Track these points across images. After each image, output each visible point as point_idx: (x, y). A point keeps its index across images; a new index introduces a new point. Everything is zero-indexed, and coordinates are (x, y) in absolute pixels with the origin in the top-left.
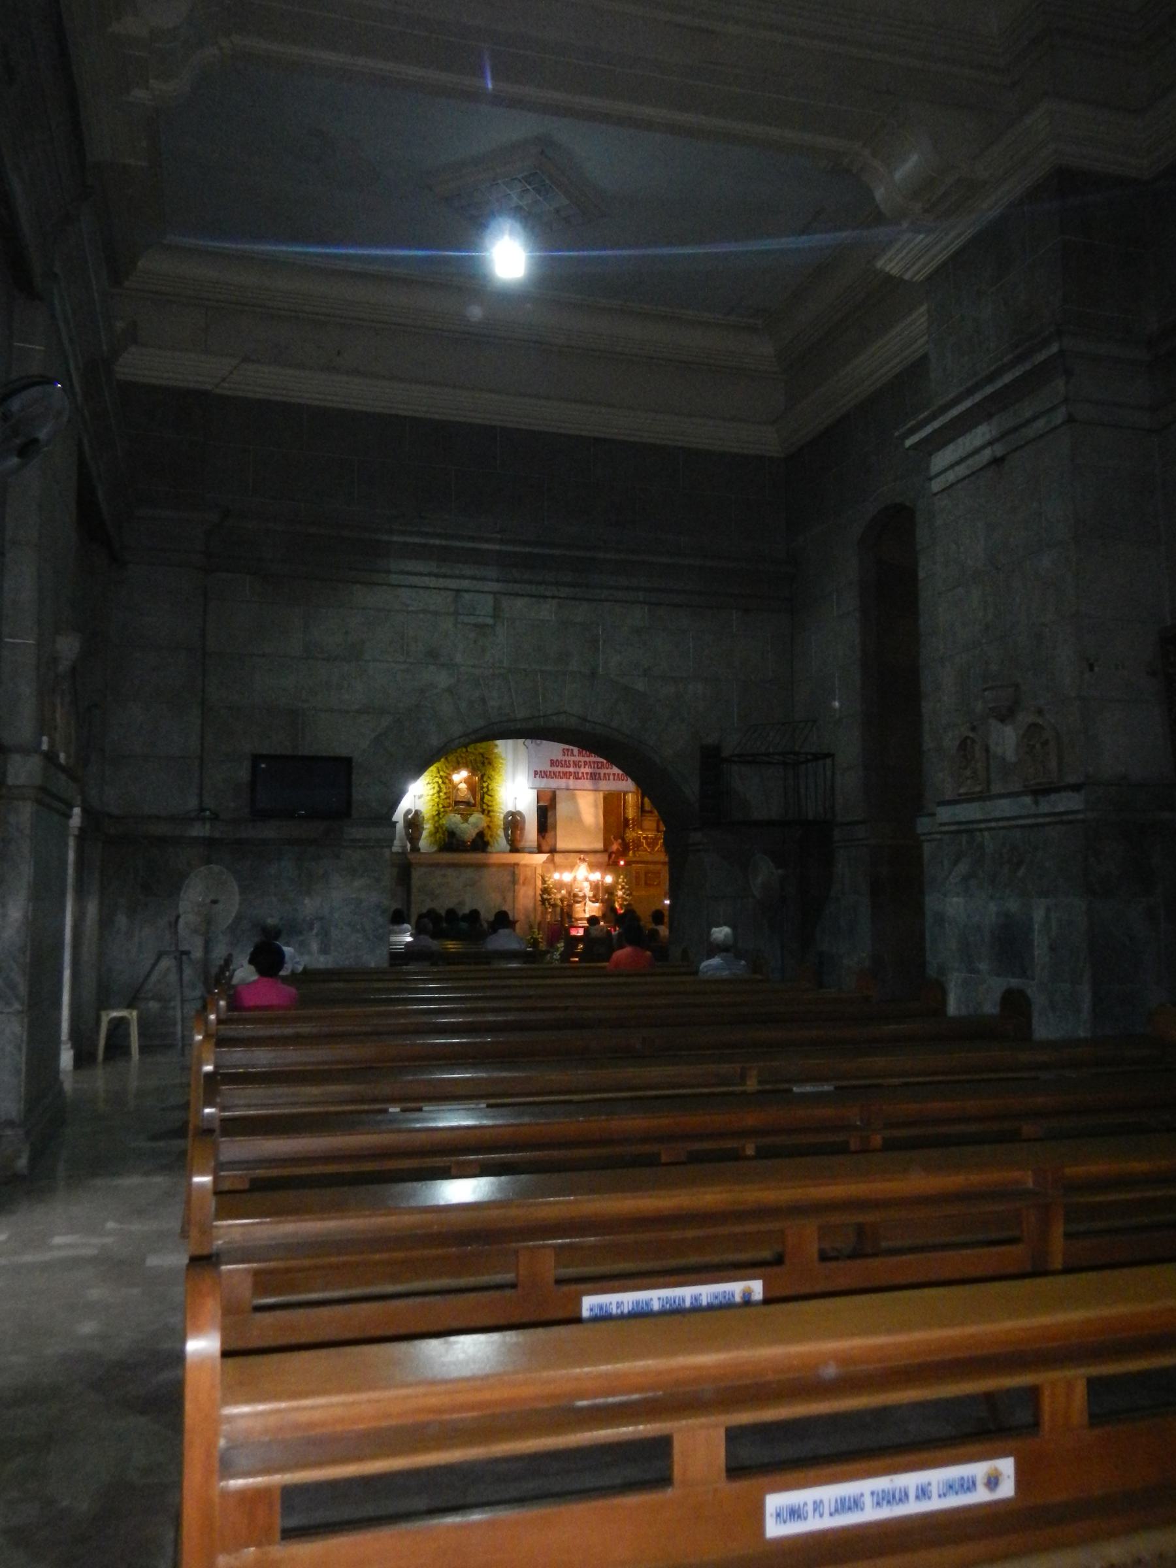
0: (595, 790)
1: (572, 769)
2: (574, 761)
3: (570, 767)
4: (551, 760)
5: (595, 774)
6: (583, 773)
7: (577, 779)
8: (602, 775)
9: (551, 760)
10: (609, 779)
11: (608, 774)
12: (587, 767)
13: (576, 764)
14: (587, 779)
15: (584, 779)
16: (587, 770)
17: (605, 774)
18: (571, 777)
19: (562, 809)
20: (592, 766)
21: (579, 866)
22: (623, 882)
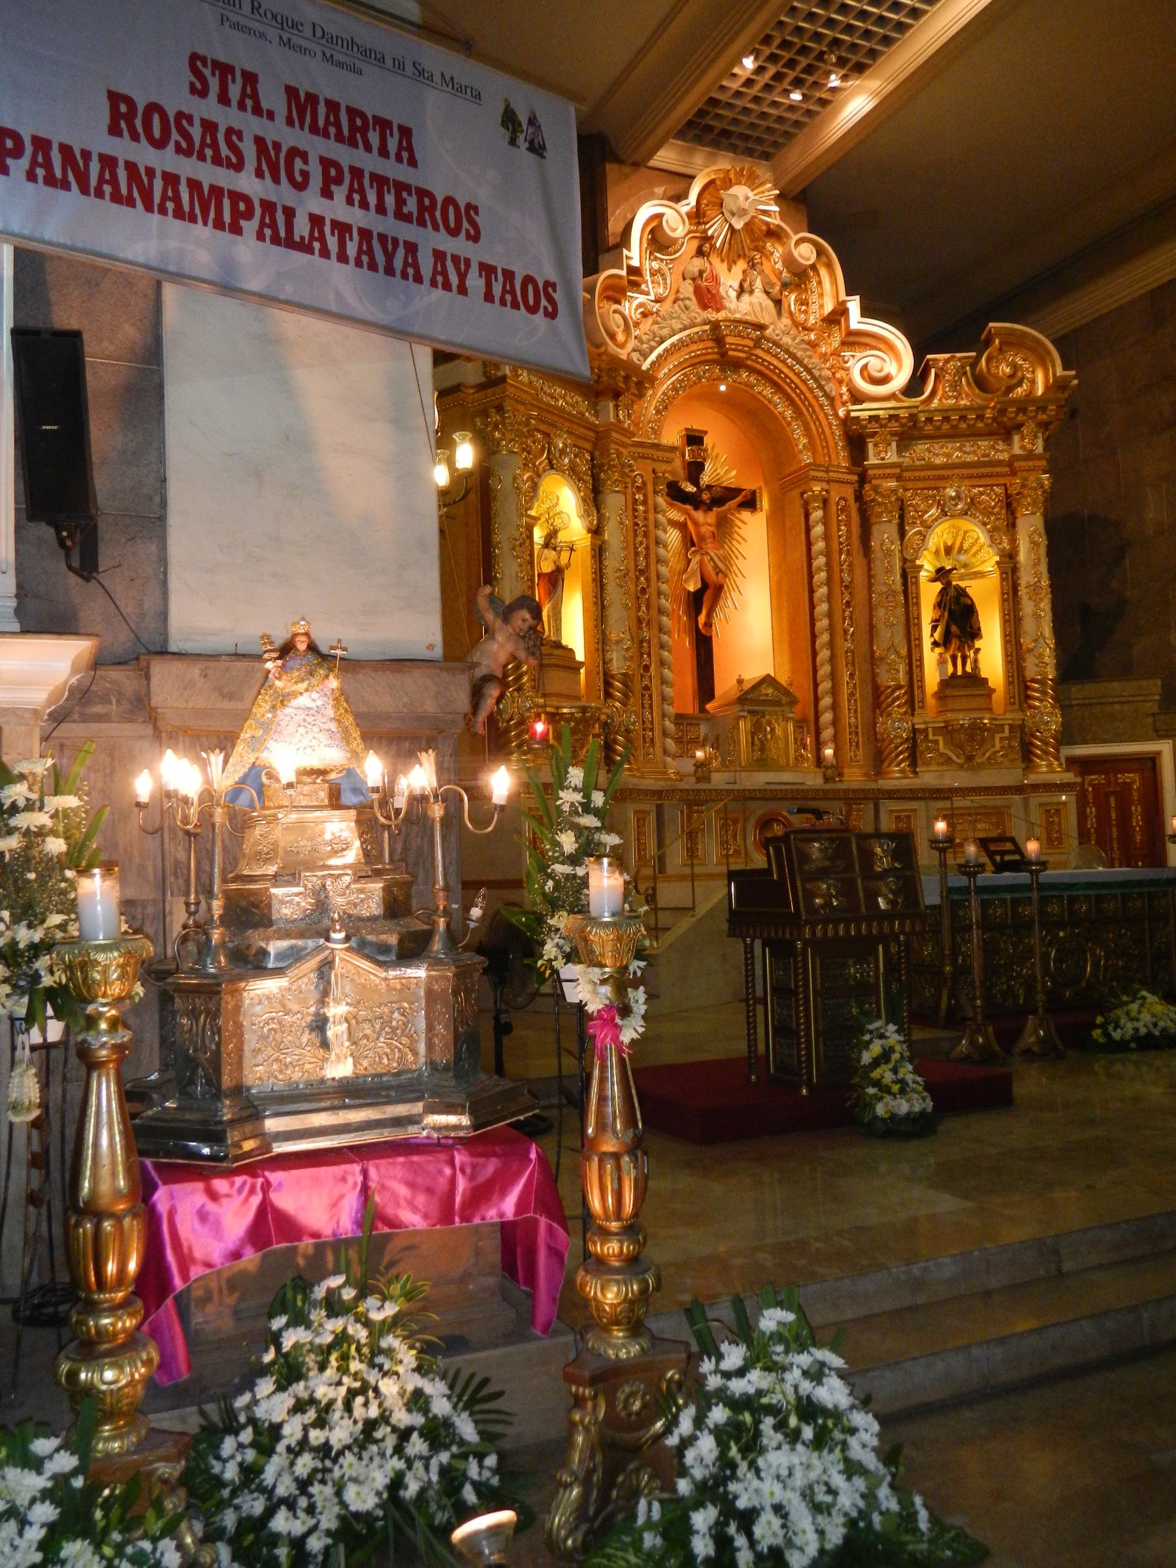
1: (248, 183)
2: (259, 141)
3: (239, 167)
4: (114, 98)
6: (316, 221)
7: (276, 240)
9: (114, 98)
10: (462, 290)
11: (456, 259)
12: (340, 193)
14: (343, 258)
15: (325, 253)
16: (337, 209)
18: (250, 227)
20: (372, 199)
21: (283, 699)
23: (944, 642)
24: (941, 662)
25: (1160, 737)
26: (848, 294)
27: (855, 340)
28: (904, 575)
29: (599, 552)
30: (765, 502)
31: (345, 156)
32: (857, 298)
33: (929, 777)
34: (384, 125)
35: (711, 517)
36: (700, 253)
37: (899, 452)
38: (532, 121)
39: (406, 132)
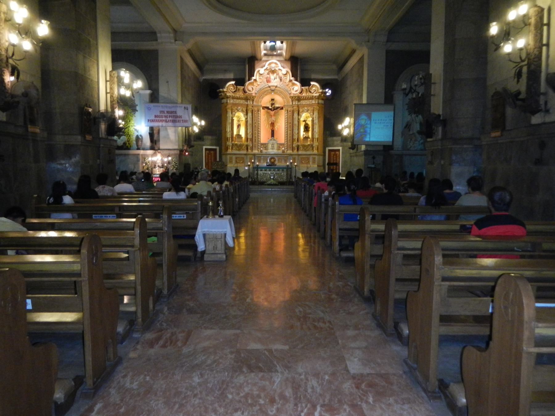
0: (175, 126)
1: (164, 119)
5: (174, 120)
6: (169, 120)
8: (177, 121)
12: (170, 118)
13: (165, 117)
16: (170, 119)
17: (178, 120)
19: (162, 133)
22: (175, 160)
23: (305, 131)
24: (304, 135)
25: (341, 146)
26: (292, 77)
27: (294, 84)
28: (298, 122)
29: (247, 122)
30: (284, 109)
31: (171, 115)
32: (293, 78)
33: (300, 152)
34: (174, 112)
35: (274, 112)
36: (268, 74)
37: (298, 102)
38: (187, 107)
39: (176, 112)
